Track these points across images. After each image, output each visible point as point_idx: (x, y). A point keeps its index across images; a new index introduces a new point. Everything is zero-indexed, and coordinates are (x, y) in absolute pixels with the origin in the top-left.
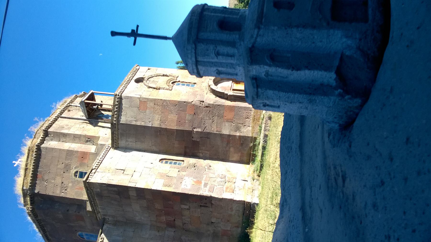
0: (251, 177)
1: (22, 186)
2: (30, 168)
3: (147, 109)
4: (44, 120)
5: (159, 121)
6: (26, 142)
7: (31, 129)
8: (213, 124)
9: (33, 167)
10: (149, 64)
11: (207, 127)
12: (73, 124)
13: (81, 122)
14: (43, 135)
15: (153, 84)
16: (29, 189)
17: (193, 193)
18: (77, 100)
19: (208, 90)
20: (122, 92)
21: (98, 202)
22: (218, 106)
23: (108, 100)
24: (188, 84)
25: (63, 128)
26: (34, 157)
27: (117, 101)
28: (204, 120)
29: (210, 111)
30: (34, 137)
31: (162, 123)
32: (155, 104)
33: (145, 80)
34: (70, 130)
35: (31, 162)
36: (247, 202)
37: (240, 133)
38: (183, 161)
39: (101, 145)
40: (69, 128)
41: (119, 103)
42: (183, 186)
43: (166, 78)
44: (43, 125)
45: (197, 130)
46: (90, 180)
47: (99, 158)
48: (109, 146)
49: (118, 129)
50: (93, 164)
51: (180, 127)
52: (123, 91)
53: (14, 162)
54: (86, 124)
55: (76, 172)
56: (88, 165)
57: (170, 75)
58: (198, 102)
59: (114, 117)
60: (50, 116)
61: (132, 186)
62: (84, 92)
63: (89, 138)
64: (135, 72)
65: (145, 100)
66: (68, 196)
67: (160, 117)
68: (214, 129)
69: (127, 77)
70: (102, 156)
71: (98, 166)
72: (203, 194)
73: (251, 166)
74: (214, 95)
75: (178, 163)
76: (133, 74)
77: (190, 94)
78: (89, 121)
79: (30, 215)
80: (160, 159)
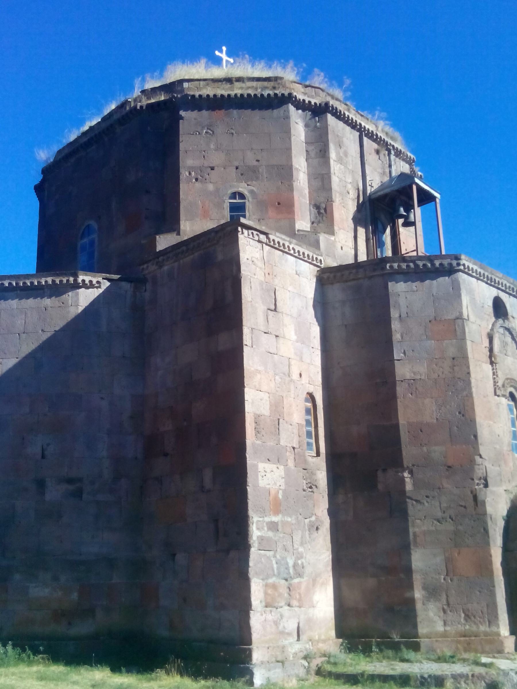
0: (311, 648)
1: (186, 78)
2: (235, 89)
3: (436, 341)
4: (346, 99)
5: (412, 375)
8: (433, 522)
9: (239, 95)
11: (419, 507)
14: (315, 103)
21: (188, 259)
22: (482, 530)
28: (437, 494)
29: (465, 507)
30: (307, 83)
31: (407, 385)
32: (453, 359)
35: (250, 89)
37: (421, 602)
38: (318, 454)
42: (262, 466)
45: (407, 480)
46: (243, 233)
49: (370, 278)
51: (407, 433)
56: (263, 219)
59: (399, 262)
60: (357, 112)
67: (423, 377)
69: (501, 275)
70: (299, 252)
71: (277, 246)
76: (511, 289)
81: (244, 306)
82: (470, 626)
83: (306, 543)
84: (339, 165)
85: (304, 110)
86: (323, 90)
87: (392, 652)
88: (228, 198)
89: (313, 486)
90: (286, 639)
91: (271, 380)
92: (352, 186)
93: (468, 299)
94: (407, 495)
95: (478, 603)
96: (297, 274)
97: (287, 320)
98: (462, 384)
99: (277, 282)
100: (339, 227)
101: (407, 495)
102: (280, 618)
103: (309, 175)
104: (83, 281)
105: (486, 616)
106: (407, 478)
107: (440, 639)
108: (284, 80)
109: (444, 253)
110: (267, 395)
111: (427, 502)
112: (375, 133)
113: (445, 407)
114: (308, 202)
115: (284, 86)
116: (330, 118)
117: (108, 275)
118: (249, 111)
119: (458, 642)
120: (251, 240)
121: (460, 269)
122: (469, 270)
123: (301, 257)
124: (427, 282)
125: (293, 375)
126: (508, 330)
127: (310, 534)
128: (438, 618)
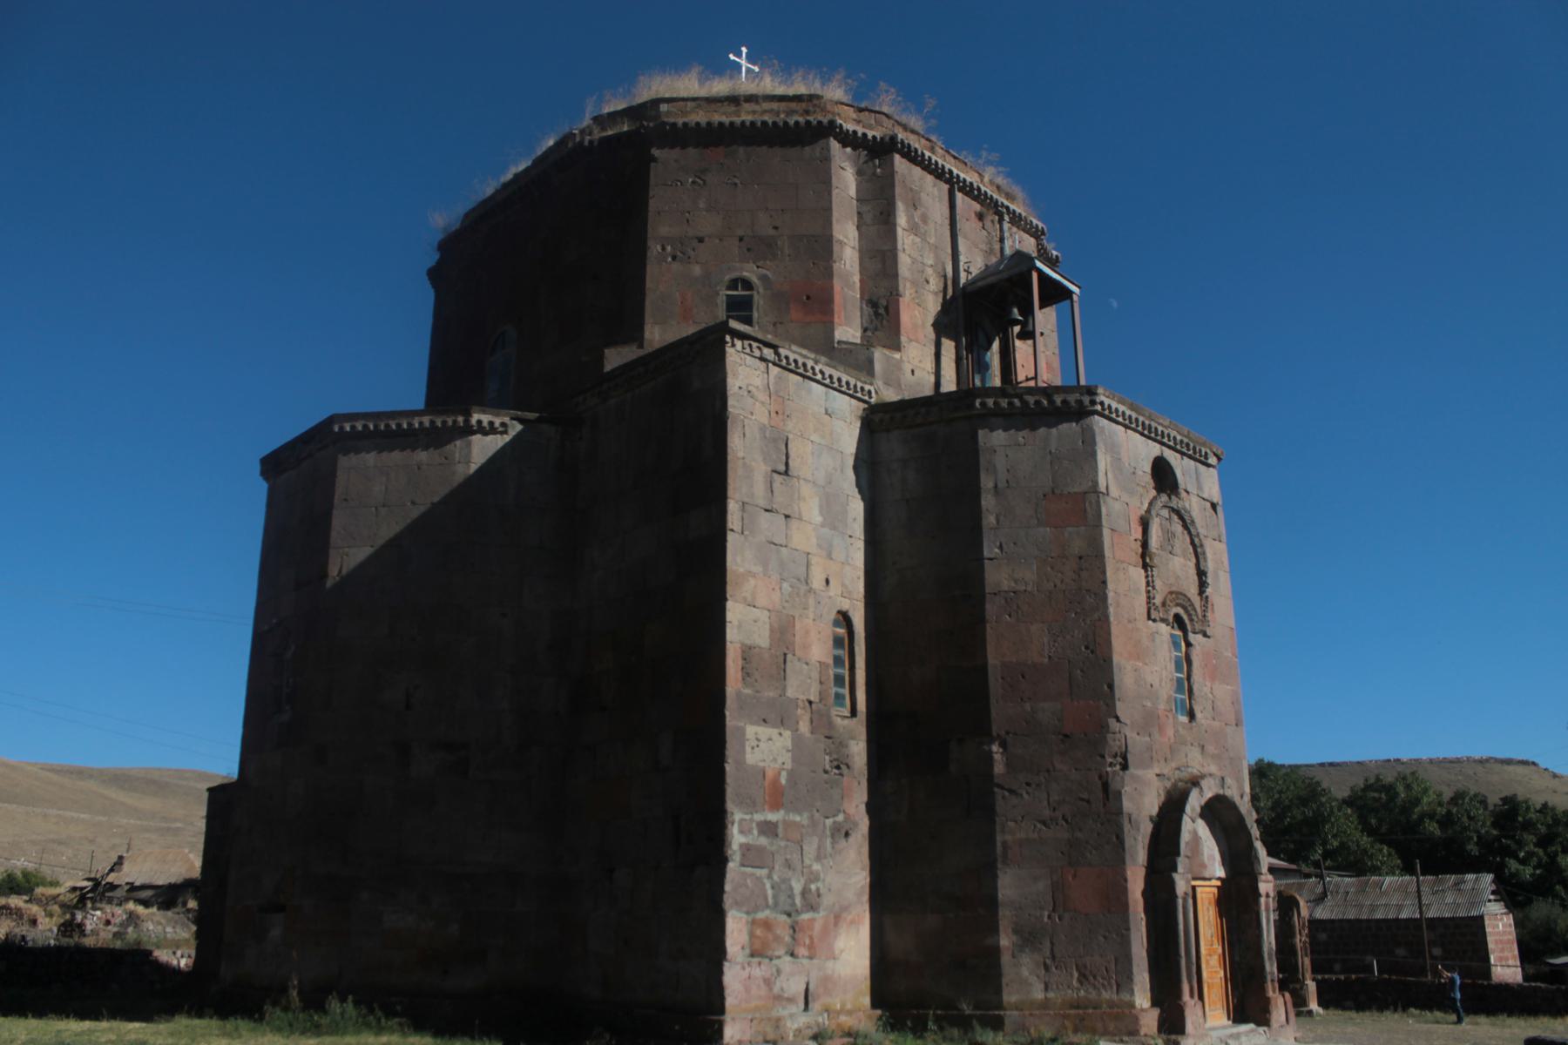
0: (827, 1022)
1: (667, 96)
2: (743, 114)
4: (929, 130)
5: (1013, 584)
6: (835, 83)
7: (887, 91)
8: (1035, 826)
9: (748, 124)
10: (1229, 505)
13: (944, 269)
14: (874, 137)
15: (1160, 534)
16: (665, 123)
17: (729, 780)
18: (1026, 236)
19: (1176, 777)
20: (1107, 412)
22: (1114, 839)
24: (1183, 684)
25: (914, 204)
26: (788, 120)
28: (1043, 780)
29: (1088, 802)
30: (863, 105)
31: (1003, 602)
33: (1170, 498)
34: (908, 233)
35: (767, 114)
36: (721, 1025)
37: (1010, 952)
38: (854, 713)
39: (871, 362)
40: (914, 229)
41: (1058, 408)
43: (1192, 591)
44: (913, 132)
45: (997, 757)
46: (733, 345)
47: (822, 367)
48: (873, 394)
50: (794, 348)
51: (1000, 680)
53: (744, 50)
54: (942, 289)
55: (748, 285)
56: (781, 323)
57: (1207, 603)
58: (1117, 742)
61: (729, 517)
62: (1060, 259)
63: (886, 309)
64: (1195, 452)
66: (652, 270)
67: (1029, 589)
68: (1012, 830)
70: (831, 377)
71: (792, 366)
72: (729, 826)
73: (870, 1017)
74: (1160, 809)
75: (840, 690)
77: (1149, 704)
78: (952, 297)
79: (560, 144)
81: (730, 465)
82: (1086, 991)
83: (825, 857)
84: (912, 237)
85: (854, 149)
86: (887, 116)
87: (959, 1031)
90: (784, 1008)
92: (935, 271)
93: (1109, 459)
94: (996, 781)
95: (1101, 956)
96: (826, 413)
97: (806, 490)
98: (1092, 600)
100: (908, 338)
101: (996, 781)
102: (776, 974)
103: (860, 251)
104: (479, 422)
105: (1114, 977)
106: (996, 753)
107: (1037, 1012)
108: (823, 101)
109: (1083, 382)
110: (766, 612)
111: (1028, 793)
112: (975, 186)
113: (1064, 638)
114: (858, 296)
115: (824, 110)
116: (899, 162)
117: (519, 413)
118: (764, 148)
119: (1065, 1017)
120: (748, 358)
122: (1111, 412)
123: (836, 385)
124: (1042, 431)
125: (814, 581)
127: (834, 843)
128: (1035, 978)
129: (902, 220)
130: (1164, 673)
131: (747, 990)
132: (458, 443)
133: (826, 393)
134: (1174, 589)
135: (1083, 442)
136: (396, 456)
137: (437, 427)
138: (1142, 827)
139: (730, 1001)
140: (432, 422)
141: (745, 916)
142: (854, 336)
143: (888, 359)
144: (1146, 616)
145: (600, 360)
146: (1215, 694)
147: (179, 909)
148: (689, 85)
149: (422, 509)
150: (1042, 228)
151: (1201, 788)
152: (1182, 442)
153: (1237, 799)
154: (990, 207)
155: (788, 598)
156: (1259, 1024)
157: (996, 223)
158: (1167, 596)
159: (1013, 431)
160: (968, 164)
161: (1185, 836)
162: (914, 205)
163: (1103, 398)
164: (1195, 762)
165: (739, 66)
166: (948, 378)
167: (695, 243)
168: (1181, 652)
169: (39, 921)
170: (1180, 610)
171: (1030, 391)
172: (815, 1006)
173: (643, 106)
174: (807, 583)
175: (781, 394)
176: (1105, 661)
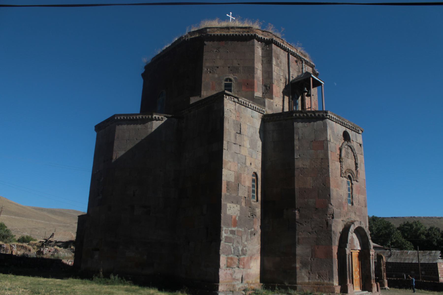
0: (247, 286)
1: (209, 27)
2: (230, 32)
3: (314, 151)
4: (282, 37)
5: (303, 166)
6: (256, 24)
7: (271, 26)
12: (283, 68)
13: (286, 77)
14: (267, 39)
15: (345, 152)
16: (208, 35)
18: (309, 67)
19: (347, 221)
20: (330, 118)
22: (329, 238)
23: (314, 101)
25: (278, 58)
26: (243, 34)
27: (320, 114)
28: (310, 221)
29: (322, 227)
30: (264, 30)
32: (322, 159)
33: (348, 143)
35: (237, 32)
36: (218, 286)
37: (299, 269)
38: (257, 200)
39: (264, 102)
40: (277, 65)
41: (317, 117)
43: (353, 169)
44: (278, 38)
45: (297, 214)
46: (226, 98)
47: (251, 104)
48: (265, 112)
50: (243, 98)
52: (331, 120)
53: (231, 13)
55: (230, 80)
56: (239, 91)
60: (287, 43)
61: (224, 145)
62: (319, 74)
64: (355, 130)
65: (325, 147)
66: (204, 76)
67: (307, 167)
68: (300, 235)
70: (253, 107)
71: (242, 104)
72: (222, 231)
74: (343, 230)
75: (254, 194)
76: (352, 128)
77: (340, 200)
78: (288, 84)
79: (179, 39)
80: (257, 173)
81: (225, 131)
82: (320, 280)
84: (277, 67)
85: (261, 42)
86: (271, 33)
87: (284, 290)
88: (224, 81)
89: (253, 215)
90: (235, 282)
91: (236, 166)
92: (283, 77)
93: (331, 131)
94: (297, 221)
95: (325, 270)
96: (252, 117)
97: (245, 138)
99: (242, 120)
100: (275, 96)
101: (297, 221)
102: (233, 272)
103: (262, 71)
104: (155, 117)
105: (328, 276)
106: (297, 213)
107: (306, 286)
108: (253, 29)
109: (324, 110)
110: (234, 172)
111: (305, 224)
114: (261, 84)
115: (253, 31)
116: (274, 46)
117: (166, 115)
118: (236, 42)
119: (314, 287)
120: (230, 101)
121: (327, 118)
122: (332, 118)
123: (255, 109)
124: (312, 123)
125: (247, 164)
126: (350, 147)
127: (251, 237)
128: (306, 276)
129: (274, 62)
130: (345, 192)
131: (226, 276)
132: (149, 123)
133: (252, 111)
134: (348, 168)
135: (323, 126)
136: (132, 126)
137: (144, 118)
138: (337, 236)
139: (221, 280)
140: (142, 117)
141: (225, 256)
142: (260, 95)
143: (269, 101)
144: (340, 176)
145: (189, 100)
146: (359, 198)
147: (69, 248)
148: (215, 24)
149: (139, 141)
150: (314, 65)
151: (354, 225)
152: (352, 127)
153: (365, 228)
154: (299, 59)
155: (240, 168)
156: (369, 291)
157: (301, 63)
158: (346, 170)
159: (304, 123)
160: (293, 47)
161: (349, 238)
162: (278, 58)
163: (329, 114)
164: (353, 217)
165: (229, 18)
166: (286, 107)
167: (216, 68)
168: (350, 186)
169: (31, 250)
170: (350, 174)
171: (309, 112)
172: (244, 282)
173: (202, 29)
174: (245, 164)
175: (239, 111)
176: (328, 188)
